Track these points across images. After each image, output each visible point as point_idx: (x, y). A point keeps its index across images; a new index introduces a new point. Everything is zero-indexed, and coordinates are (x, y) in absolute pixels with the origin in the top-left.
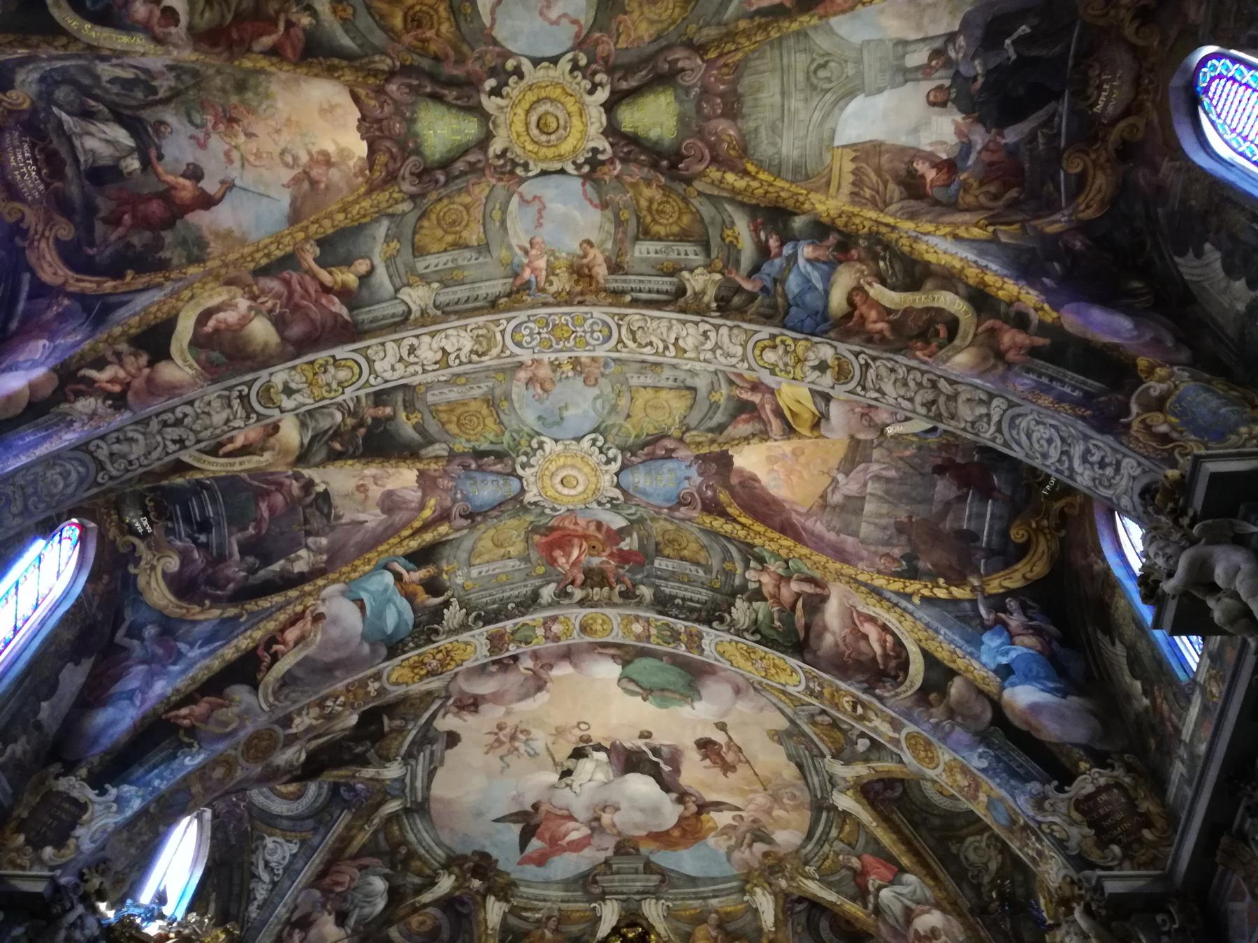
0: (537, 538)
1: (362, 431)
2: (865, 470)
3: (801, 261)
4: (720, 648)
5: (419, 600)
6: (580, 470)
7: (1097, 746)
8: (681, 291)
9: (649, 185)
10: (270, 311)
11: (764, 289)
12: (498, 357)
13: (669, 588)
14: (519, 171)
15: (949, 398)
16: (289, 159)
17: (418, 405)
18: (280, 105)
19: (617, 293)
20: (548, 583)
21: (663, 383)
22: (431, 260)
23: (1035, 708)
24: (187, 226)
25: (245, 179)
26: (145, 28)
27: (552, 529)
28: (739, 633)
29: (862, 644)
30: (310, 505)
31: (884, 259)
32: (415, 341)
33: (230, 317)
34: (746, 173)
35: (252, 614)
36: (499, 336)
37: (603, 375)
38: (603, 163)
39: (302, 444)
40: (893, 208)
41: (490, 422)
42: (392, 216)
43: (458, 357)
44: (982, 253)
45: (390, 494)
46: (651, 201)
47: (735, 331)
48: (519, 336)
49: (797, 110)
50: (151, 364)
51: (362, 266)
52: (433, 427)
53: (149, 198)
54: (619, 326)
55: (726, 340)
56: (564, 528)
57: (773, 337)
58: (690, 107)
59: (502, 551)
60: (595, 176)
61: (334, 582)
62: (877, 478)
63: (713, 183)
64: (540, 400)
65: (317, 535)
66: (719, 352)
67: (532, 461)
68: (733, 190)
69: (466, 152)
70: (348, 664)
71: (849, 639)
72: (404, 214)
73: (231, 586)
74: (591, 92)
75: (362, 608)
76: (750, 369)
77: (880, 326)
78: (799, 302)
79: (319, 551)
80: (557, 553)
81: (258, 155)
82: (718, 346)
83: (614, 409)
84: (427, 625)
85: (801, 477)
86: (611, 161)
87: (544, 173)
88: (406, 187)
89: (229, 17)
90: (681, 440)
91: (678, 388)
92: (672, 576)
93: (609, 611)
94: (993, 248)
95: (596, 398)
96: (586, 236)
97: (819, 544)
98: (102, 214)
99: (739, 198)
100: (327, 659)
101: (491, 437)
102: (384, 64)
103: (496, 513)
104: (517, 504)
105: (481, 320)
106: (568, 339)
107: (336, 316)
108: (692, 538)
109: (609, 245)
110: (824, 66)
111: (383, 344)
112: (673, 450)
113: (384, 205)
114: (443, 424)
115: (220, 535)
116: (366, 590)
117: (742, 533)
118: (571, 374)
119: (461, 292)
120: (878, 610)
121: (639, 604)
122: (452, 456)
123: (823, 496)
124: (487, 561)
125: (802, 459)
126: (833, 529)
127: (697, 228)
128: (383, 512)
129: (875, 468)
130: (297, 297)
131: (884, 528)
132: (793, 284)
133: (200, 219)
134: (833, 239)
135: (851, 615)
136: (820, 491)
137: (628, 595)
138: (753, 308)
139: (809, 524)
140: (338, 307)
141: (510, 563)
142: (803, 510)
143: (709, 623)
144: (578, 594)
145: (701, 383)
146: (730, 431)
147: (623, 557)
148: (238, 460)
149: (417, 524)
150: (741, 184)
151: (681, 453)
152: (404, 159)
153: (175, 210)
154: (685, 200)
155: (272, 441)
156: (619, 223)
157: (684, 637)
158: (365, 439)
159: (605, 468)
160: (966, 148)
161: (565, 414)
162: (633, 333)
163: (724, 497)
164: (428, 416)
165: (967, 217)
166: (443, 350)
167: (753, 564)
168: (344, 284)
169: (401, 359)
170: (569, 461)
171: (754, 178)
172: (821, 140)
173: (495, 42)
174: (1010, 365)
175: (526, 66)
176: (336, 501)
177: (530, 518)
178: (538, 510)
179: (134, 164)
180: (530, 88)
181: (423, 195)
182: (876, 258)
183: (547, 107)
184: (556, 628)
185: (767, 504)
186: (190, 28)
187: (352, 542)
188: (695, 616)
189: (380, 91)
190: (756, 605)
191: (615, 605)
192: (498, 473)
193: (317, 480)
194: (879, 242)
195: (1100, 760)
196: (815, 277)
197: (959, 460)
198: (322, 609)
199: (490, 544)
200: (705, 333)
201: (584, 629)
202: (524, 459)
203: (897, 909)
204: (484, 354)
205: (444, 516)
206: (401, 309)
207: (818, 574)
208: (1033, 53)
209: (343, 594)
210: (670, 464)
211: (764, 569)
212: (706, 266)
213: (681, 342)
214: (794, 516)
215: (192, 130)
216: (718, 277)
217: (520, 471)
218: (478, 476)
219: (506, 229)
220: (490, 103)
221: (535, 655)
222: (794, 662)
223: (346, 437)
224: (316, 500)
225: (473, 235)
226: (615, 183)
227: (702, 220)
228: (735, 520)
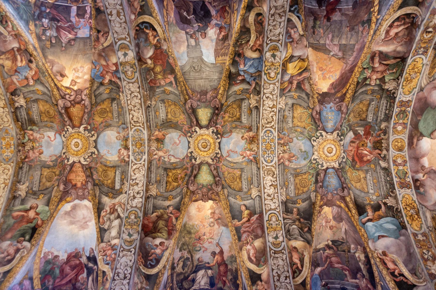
0: (357, 166)
1: (302, 220)
2: (329, 45)
3: (245, 69)
4: (407, 93)
5: (382, 214)
6: (325, 146)
9: (224, 117)
10: (253, 239)
11: (254, 80)
12: (275, 168)
13: (382, 116)
14: (219, 156)
15: (276, 9)
16: (212, 224)
17: (294, 199)
18: (196, 223)
20: (379, 164)
21: (291, 115)
22: (244, 187)
24: (227, 260)
25: (216, 238)
26: (163, 251)
27: (353, 160)
28: (398, 85)
29: (400, 34)
30: (337, 248)
31: (241, 42)
32: (266, 194)
33: (252, 252)
35: (380, 281)
36: (268, 167)
37: (288, 136)
38: (217, 131)
39: (303, 241)
41: (304, 177)
42: (228, 196)
43: (274, 181)
45: (334, 218)
46: (229, 117)
47: (265, 87)
48: (269, 162)
49: (206, 75)
51: (243, 208)
52: (305, 196)
53: (219, 270)
54: (266, 127)
55: (268, 90)
56: (353, 155)
57: (265, 73)
58: (203, 105)
59: (362, 180)
60: (221, 133)
61: (368, 244)
62: (332, 40)
63: (222, 97)
64: (298, 158)
65: (350, 248)
66: (273, 93)
67: (321, 163)
68: (224, 90)
69: (211, 170)
70: (408, 246)
71: (398, 40)
72: (228, 192)
73: (369, 286)
74: (197, 132)
75: (383, 236)
76: (278, 82)
79: (357, 249)
80: (365, 159)
81: (210, 233)
82: (271, 93)
83: (302, 133)
84: (394, 212)
85: (332, 67)
86: (217, 128)
87: (220, 148)
88: (220, 189)
89: (166, 228)
90: (313, 109)
91: (293, 110)
92: (376, 114)
93: (391, 140)
95: (298, 139)
96: (240, 138)
97: (357, 58)
98: (222, 286)
99: (227, 89)
100: (406, 254)
101: (310, 177)
102: (185, 189)
103: (343, 179)
104: (340, 172)
105: (262, 172)
106: (271, 145)
107: (257, 219)
108: (357, 106)
109: (243, 131)
110: (194, 68)
111: (265, 204)
112: (317, 112)
113: (224, 197)
114: (303, 192)
115: (348, 285)
116: (374, 233)
117: (352, 86)
118: (288, 147)
119: (255, 179)
120: (382, 30)
121: (387, 127)
122: (316, 191)
123: (340, 59)
124: (367, 186)
125: (324, 68)
126: (352, 53)
127: (237, 102)
128: (342, 222)
129: (328, 42)
130: (249, 230)
131: (352, 35)
132: (252, 70)
133: (226, 255)
134: (237, 59)
135: (387, 40)
136: (337, 60)
137: (385, 132)
139: (350, 63)
140: (254, 218)
141: (368, 177)
142: (345, 65)
143: (395, 98)
144: (385, 152)
145: (290, 102)
146: (308, 91)
147: (367, 134)
148: (305, 263)
149: (347, 209)
150: (222, 88)
151: (318, 108)
152: (213, 190)
153: (222, 263)
154: (228, 106)
155: (300, 251)
156: (236, 127)
157: (403, 109)
158: (305, 219)
159: (324, 137)
160: (216, 25)
161: (303, 150)
162: (268, 123)
163: (339, 95)
164: (300, 197)
166: (270, 186)
167: (368, 82)
168: (248, 215)
169: (272, 200)
170: (321, 150)
172: (214, 67)
173: (184, 159)
175: (190, 150)
176: (336, 238)
177: (347, 167)
178: (344, 164)
179: (210, 272)
180: (195, 149)
181: (223, 185)
182: (241, 44)
183: (200, 145)
184: (399, 161)
185: (342, 79)
186: (166, 239)
187: (353, 235)
188: (392, 104)
189: (193, 193)
190: (387, 80)
191: (389, 137)
192: (325, 175)
193: (327, 243)
194: (236, 43)
196: (249, 63)
197: (325, 13)
198: (380, 251)
199: (359, 184)
200: (267, 98)
201: (400, 149)
202: (320, 166)
204: (274, 173)
205: (343, 199)
206: (257, 198)
207: (369, 56)
208: (192, 10)
209: (374, 242)
210: (324, 113)
211: (370, 78)
212: (249, 100)
213: (271, 106)
214: (347, 69)
215: (201, 251)
216: (251, 96)
217: (325, 168)
218: (326, 184)
219: (237, 163)
220: (198, 162)
221: (417, 172)
222: (409, 61)
223: (303, 226)
224: (335, 246)
225: (238, 173)
226: (224, 128)
227: (235, 101)
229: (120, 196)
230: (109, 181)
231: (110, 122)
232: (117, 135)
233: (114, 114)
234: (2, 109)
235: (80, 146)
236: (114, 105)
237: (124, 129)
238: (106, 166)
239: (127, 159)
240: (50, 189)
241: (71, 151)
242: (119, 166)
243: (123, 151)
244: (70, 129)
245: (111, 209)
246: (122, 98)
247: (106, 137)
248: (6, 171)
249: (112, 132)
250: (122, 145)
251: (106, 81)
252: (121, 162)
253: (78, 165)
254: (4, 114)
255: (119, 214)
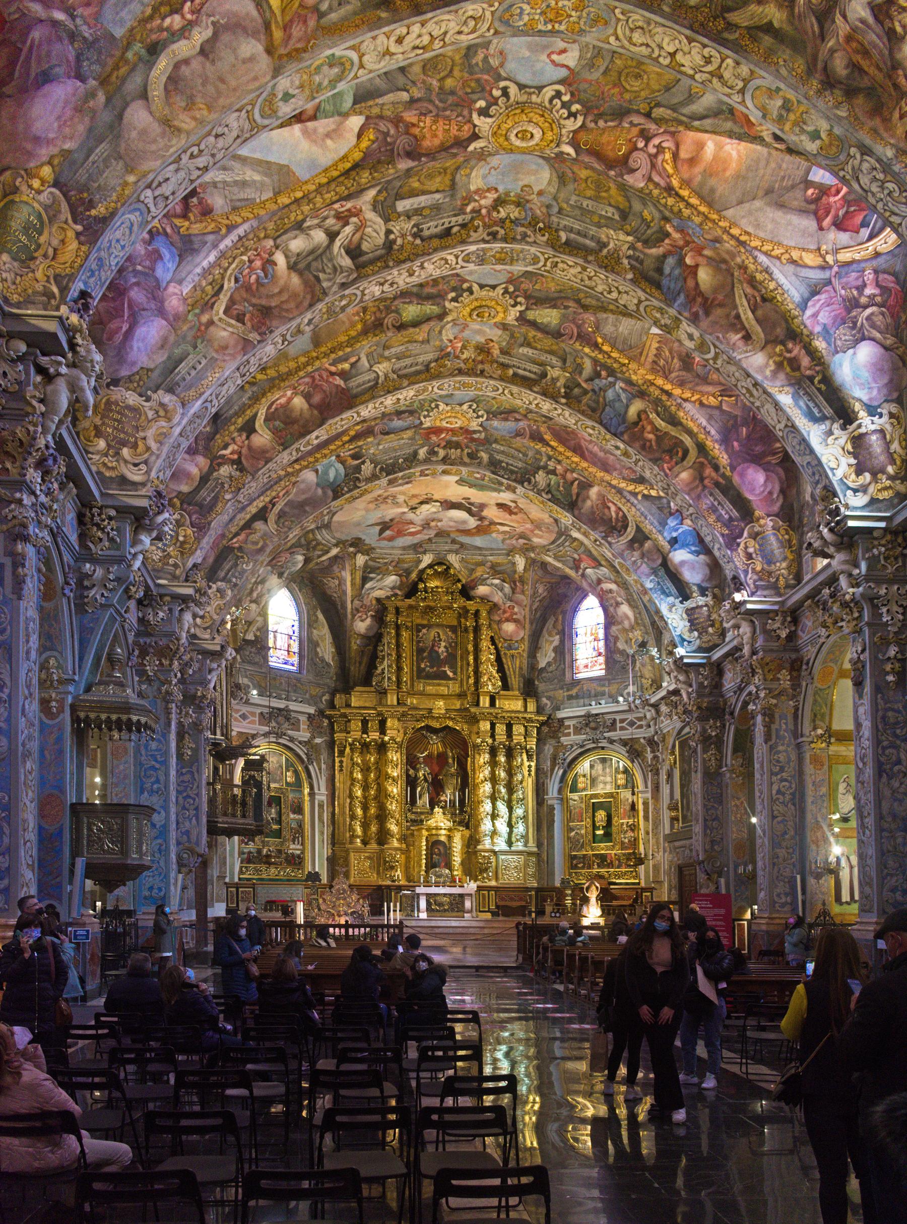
7: (705, 585)
8: (544, 375)
19: (505, 366)
23: (683, 563)
34: (596, 346)
40: (673, 375)
44: (710, 418)
50: (248, 438)
77: (651, 436)
78: (611, 404)
94: (716, 413)
132: (610, 394)
138: (585, 400)
156: (512, 336)
165: (710, 389)
171: (601, 351)
174: (704, 487)
175: (476, 288)
195: (703, 592)
196: (623, 396)
203: (594, 578)
228: (548, 445)
229: (379, 220)
230: (416, 185)
231: (571, 187)
232: (536, 189)
233: (590, 202)
234: (671, 50)
235: (518, 143)
236: (610, 212)
237: (548, 207)
238: (458, 168)
239: (469, 209)
240: (401, 80)
241: (510, 123)
242: (452, 196)
243: (492, 196)
244: (572, 125)
245: (349, 210)
246: (622, 237)
247: (534, 167)
248: (472, 23)
249: (545, 182)
250: (507, 194)
251: (669, 228)
252: (464, 199)
253: (466, 130)
254: (653, 45)
255: (338, 233)
